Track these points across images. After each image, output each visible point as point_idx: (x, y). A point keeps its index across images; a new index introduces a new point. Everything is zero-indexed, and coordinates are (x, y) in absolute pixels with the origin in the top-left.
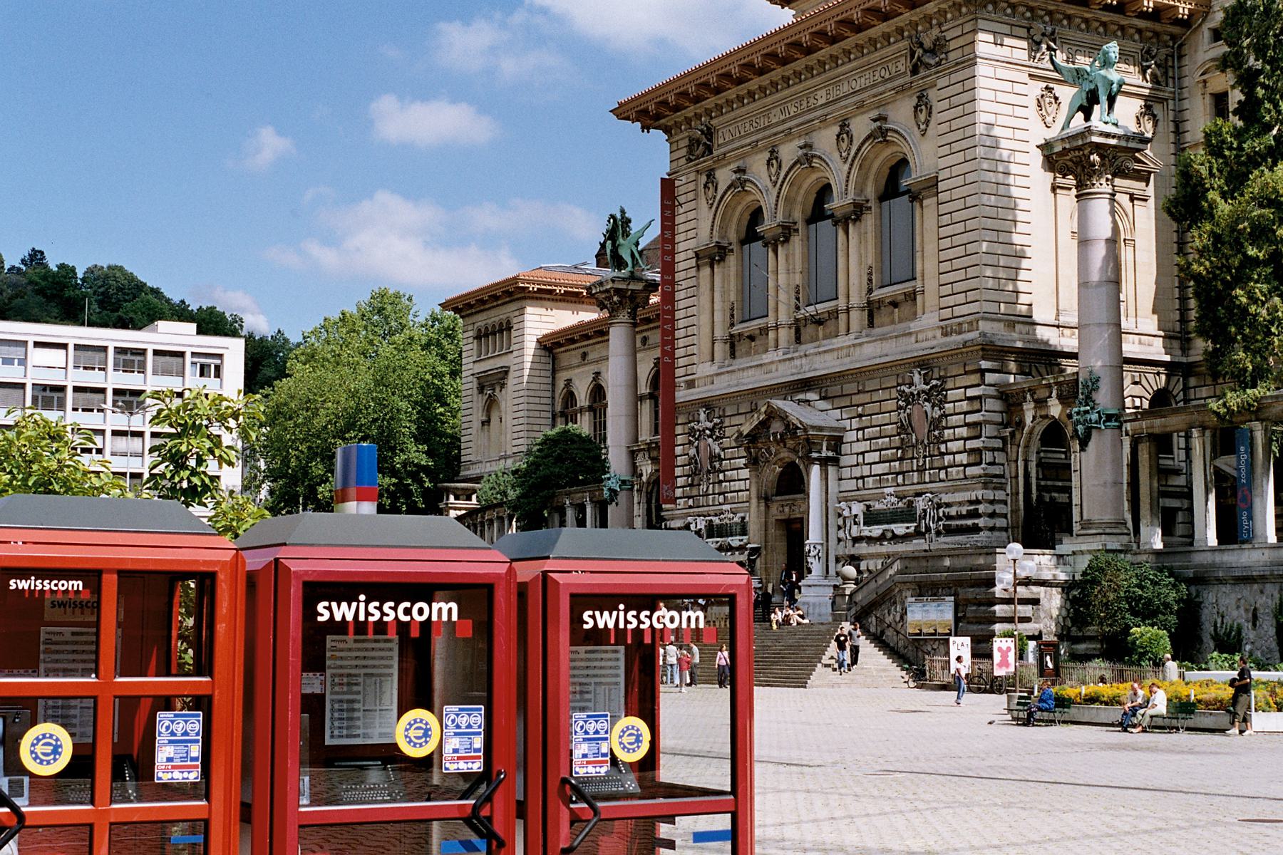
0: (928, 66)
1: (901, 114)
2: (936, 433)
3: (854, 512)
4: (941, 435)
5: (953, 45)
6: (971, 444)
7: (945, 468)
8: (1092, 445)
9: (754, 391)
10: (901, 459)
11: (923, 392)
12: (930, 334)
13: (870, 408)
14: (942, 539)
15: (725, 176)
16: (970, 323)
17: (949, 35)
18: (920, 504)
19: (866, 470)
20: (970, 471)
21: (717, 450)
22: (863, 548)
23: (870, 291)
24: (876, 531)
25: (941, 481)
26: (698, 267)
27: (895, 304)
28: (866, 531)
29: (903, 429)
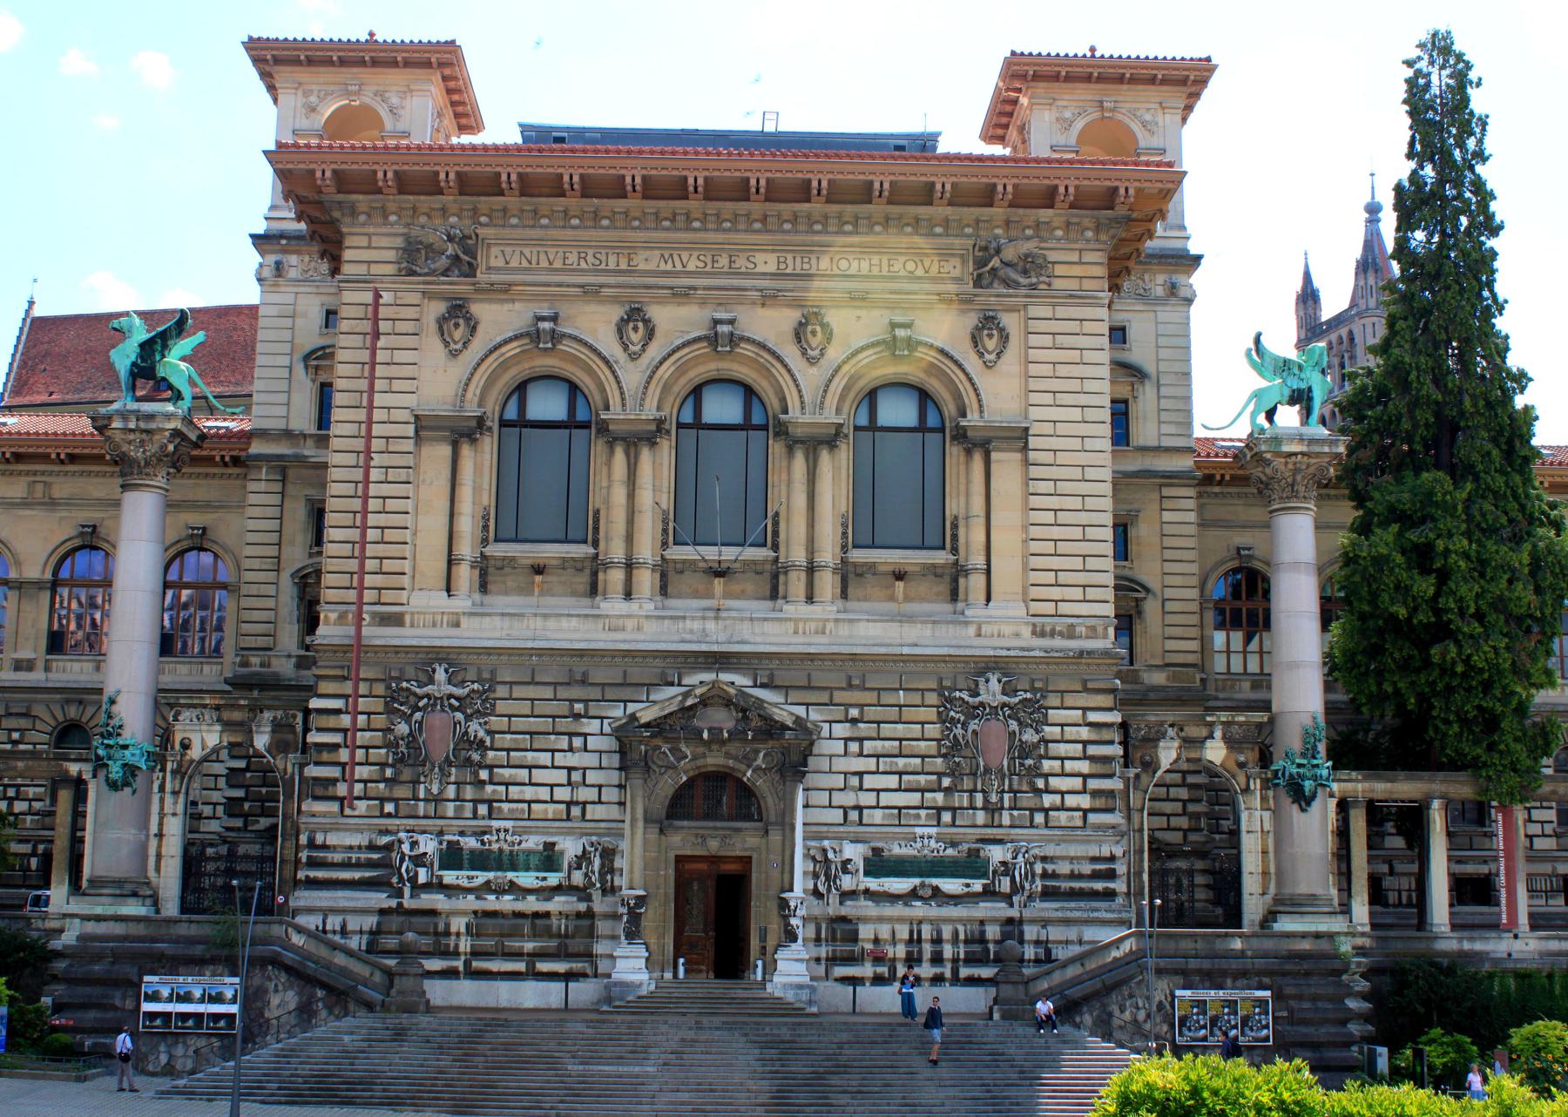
0: (1008, 283)
2: (1029, 762)
3: (847, 855)
4: (1037, 767)
5: (1059, 270)
6: (1093, 784)
7: (1046, 811)
8: (1316, 805)
9: (581, 653)
10: (948, 791)
11: (1004, 705)
12: (1007, 630)
13: (871, 712)
14: (1038, 904)
15: (498, 320)
16: (1093, 628)
17: (1053, 256)
19: (868, 799)
20: (1092, 818)
21: (481, 734)
22: (866, 907)
23: (844, 548)
24: (900, 885)
25: (1032, 826)
26: (418, 438)
27: (900, 576)
28: (873, 884)
29: (951, 748)
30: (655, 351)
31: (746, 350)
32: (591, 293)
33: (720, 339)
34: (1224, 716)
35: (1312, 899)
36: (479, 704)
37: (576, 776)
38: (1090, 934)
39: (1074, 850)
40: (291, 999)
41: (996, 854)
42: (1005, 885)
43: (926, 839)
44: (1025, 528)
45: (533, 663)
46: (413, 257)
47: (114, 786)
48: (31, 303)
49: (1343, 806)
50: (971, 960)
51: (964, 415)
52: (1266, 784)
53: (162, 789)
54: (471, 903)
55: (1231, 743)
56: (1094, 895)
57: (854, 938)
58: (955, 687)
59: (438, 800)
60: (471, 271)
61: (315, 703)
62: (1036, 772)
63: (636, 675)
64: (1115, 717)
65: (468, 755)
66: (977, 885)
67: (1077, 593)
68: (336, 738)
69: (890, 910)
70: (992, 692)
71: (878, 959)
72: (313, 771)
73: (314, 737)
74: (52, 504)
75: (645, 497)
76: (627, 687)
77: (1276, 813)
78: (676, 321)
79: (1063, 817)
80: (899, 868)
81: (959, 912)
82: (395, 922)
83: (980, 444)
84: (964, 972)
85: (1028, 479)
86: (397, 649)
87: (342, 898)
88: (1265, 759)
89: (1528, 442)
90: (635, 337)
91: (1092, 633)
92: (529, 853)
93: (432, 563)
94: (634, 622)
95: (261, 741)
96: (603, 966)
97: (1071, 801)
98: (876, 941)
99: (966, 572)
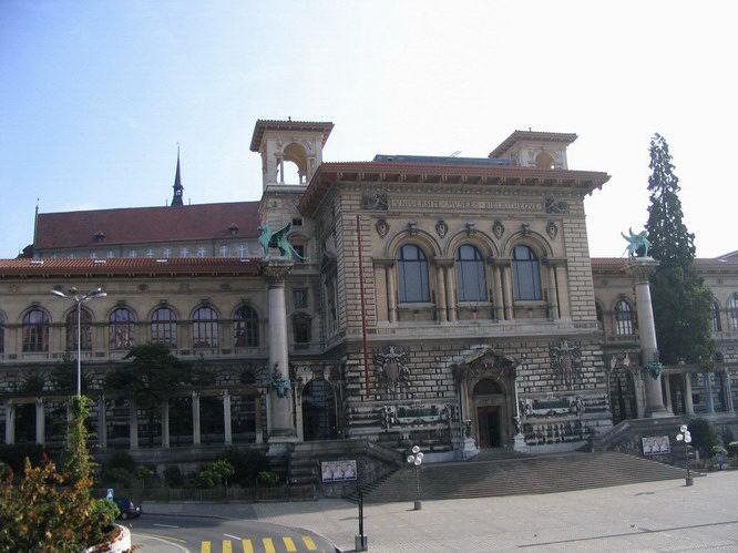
1: (539, 227)
6: (597, 375)
15: (396, 225)
17: (569, 202)
18: (571, 399)
19: (531, 384)
24: (544, 411)
27: (530, 309)
29: (554, 366)
30: (449, 234)
31: (478, 234)
32: (426, 215)
33: (468, 230)
34: (629, 350)
35: (660, 407)
36: (405, 360)
37: (439, 383)
38: (600, 422)
39: (593, 396)
40: (372, 466)
41: (571, 399)
42: (575, 409)
43: (550, 396)
44: (569, 292)
45: (421, 344)
46: (366, 203)
47: (281, 396)
48: (37, 208)
49: (662, 378)
50: (567, 434)
51: (546, 255)
52: (644, 371)
53: (293, 395)
54: (409, 428)
55: (632, 359)
56: (599, 410)
57: (531, 430)
58: (554, 344)
59: (394, 394)
60: (385, 208)
61: (349, 362)
62: (580, 372)
63: (455, 347)
64: (601, 353)
65: (403, 378)
66: (567, 410)
67: (586, 313)
68: (358, 374)
69: (541, 420)
70: (565, 346)
71: (540, 436)
72: (350, 386)
73: (350, 374)
74: (190, 292)
75: (452, 286)
76: (452, 351)
77: (645, 381)
78: (454, 225)
79: (589, 386)
80: (543, 406)
81: (564, 418)
82: (385, 437)
83: (552, 265)
84: (565, 438)
85: (568, 277)
86: (375, 342)
87: (367, 430)
88: (641, 364)
89: (691, 259)
90: (443, 231)
91: (592, 325)
92: (427, 410)
93: (383, 311)
94: (452, 328)
95: (327, 377)
96: (455, 447)
97: (591, 380)
98: (538, 431)
99: (551, 307)
